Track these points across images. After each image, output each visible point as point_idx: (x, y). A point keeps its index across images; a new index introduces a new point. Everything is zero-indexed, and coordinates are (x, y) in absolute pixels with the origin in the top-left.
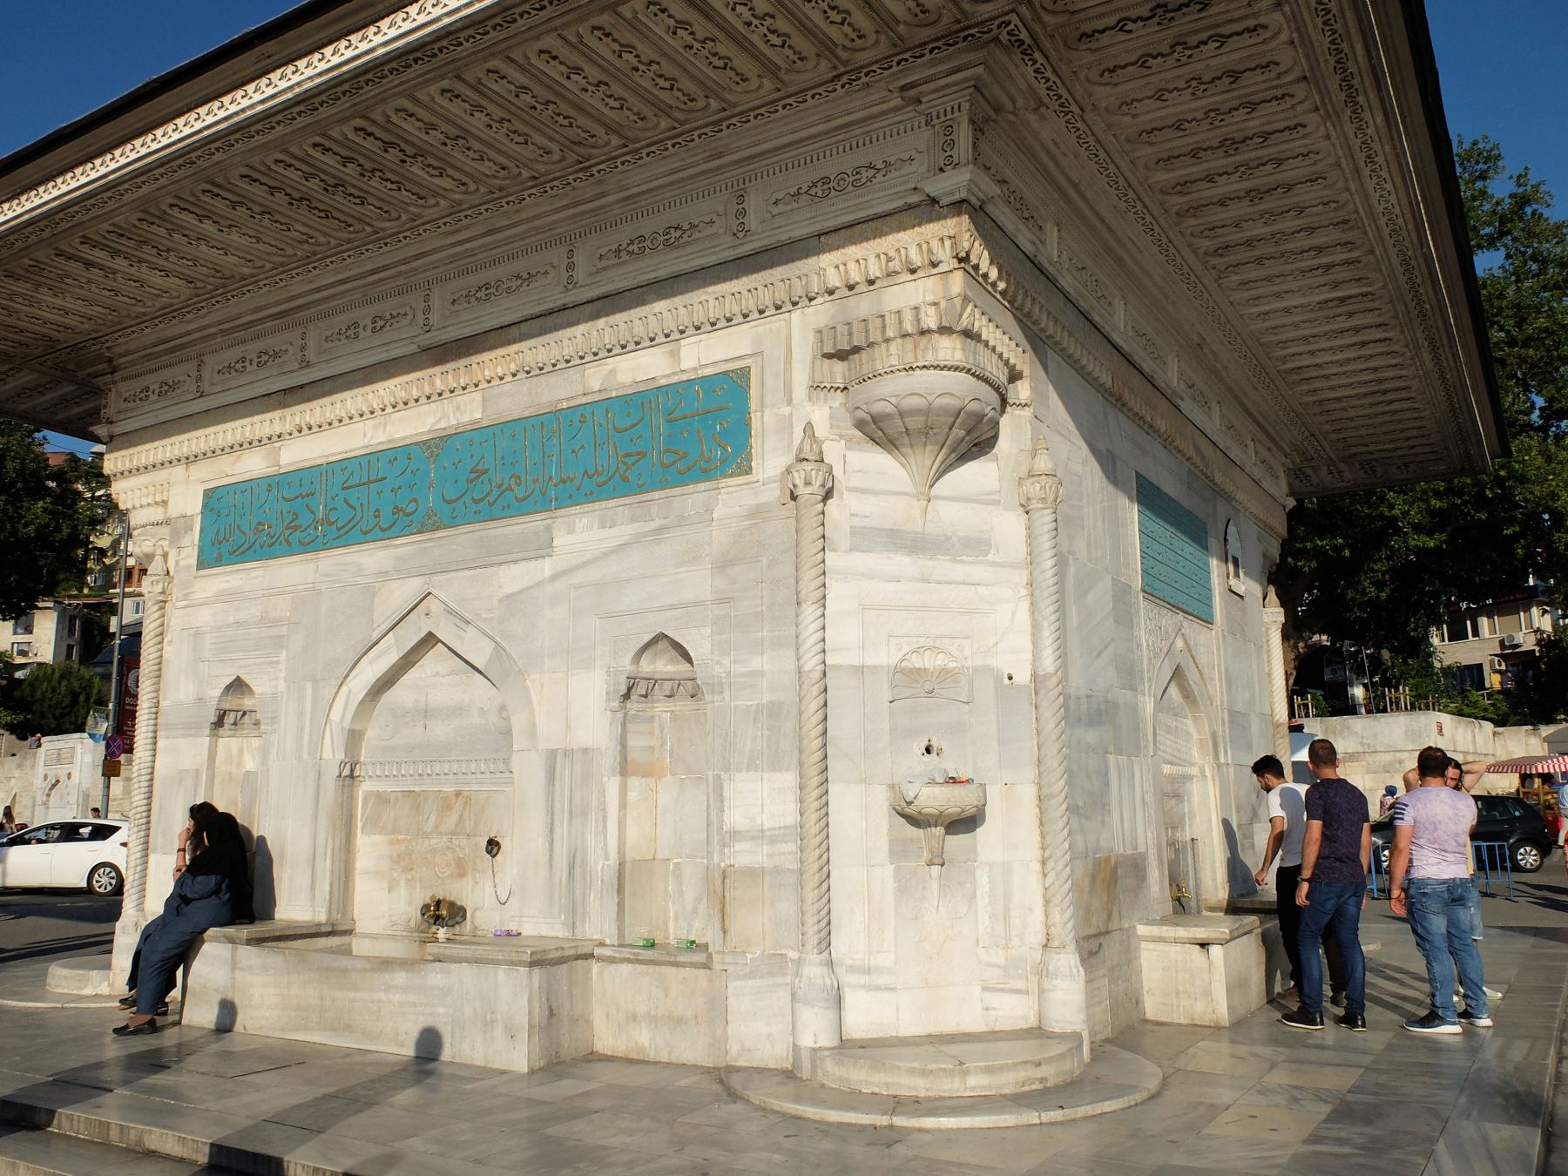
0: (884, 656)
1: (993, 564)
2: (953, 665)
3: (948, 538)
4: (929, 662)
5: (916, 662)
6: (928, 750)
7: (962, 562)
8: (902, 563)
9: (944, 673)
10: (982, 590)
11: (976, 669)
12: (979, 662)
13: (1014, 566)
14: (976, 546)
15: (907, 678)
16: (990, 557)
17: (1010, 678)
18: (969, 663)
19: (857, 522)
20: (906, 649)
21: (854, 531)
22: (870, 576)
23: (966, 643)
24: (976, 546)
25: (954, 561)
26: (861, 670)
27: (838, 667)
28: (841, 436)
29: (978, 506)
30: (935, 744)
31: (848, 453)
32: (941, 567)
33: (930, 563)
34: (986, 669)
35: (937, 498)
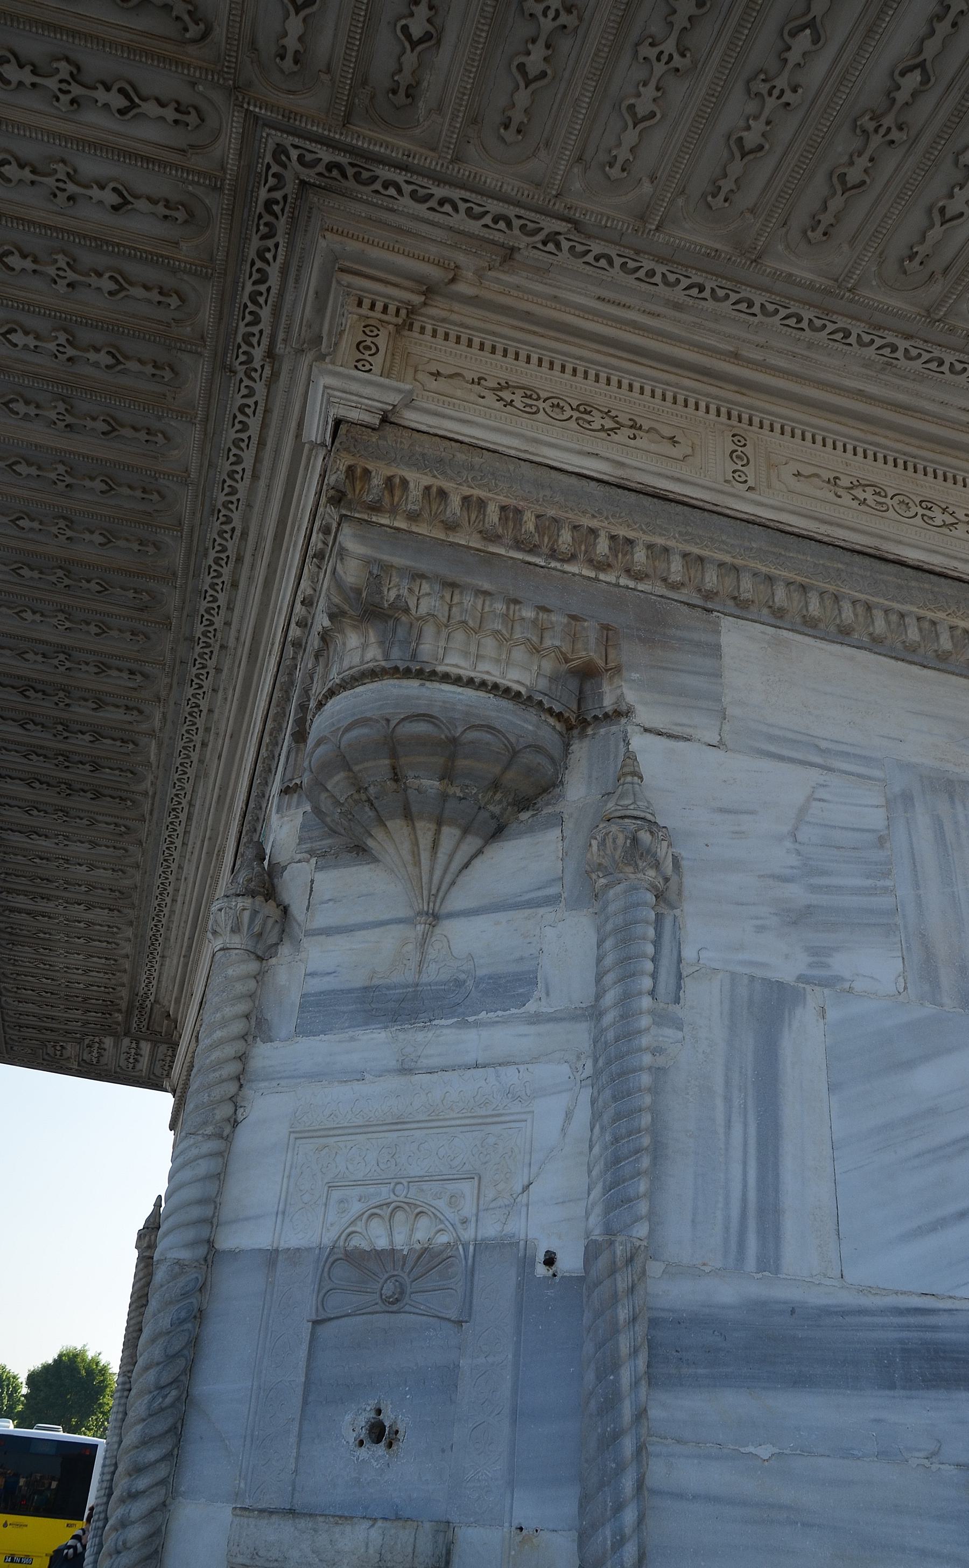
0: (310, 1231)
1: (536, 1019)
2: (443, 1239)
3: (459, 983)
4: (403, 1236)
5: (377, 1237)
6: (378, 1432)
7: (477, 1024)
8: (375, 1044)
9: (430, 1260)
10: (510, 1075)
11: (481, 1246)
12: (490, 1229)
13: (574, 1017)
14: (508, 989)
15: (353, 1266)
16: (531, 1007)
17: (550, 1260)
18: (468, 1234)
19: (316, 985)
20: (356, 1208)
21: (310, 1003)
22: (316, 1076)
23: (467, 1188)
24: (508, 989)
25: (464, 1024)
26: (271, 1257)
27: (234, 1254)
28: (312, 853)
29: (519, 915)
30: (387, 1419)
31: (319, 876)
32: (444, 1040)
33: (420, 1036)
34: (504, 1244)
35: (451, 915)
